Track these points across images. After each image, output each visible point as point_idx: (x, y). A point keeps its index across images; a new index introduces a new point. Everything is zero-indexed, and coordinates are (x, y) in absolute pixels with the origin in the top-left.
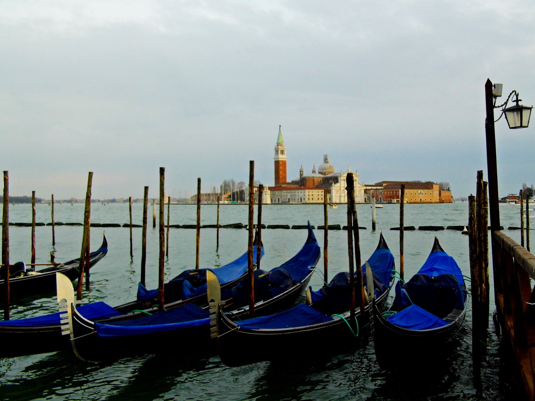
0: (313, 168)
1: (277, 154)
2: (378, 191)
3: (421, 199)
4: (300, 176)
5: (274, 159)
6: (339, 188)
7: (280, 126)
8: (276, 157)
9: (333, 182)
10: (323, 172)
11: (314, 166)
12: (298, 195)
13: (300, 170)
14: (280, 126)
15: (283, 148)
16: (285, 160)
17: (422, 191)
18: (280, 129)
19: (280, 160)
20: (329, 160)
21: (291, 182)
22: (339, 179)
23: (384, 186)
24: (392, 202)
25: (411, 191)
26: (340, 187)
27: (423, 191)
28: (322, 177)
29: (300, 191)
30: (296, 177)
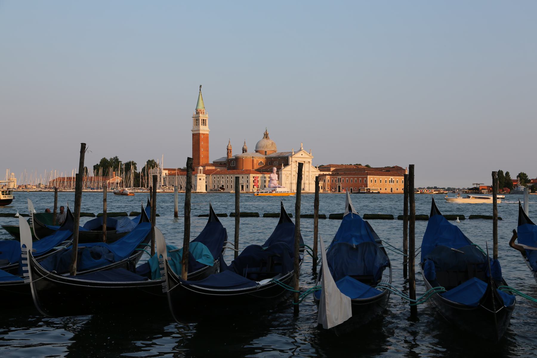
1: (197, 125)
2: (336, 178)
3: (392, 189)
4: (228, 155)
5: (192, 131)
6: (290, 172)
7: (201, 86)
8: (195, 129)
9: (283, 165)
10: (263, 151)
11: (245, 142)
13: (228, 147)
14: (201, 86)
15: (205, 116)
16: (208, 133)
17: (393, 178)
18: (200, 90)
19: (201, 132)
21: (213, 163)
22: (290, 159)
23: (332, 171)
24: (361, 192)
25: (381, 178)
27: (394, 178)
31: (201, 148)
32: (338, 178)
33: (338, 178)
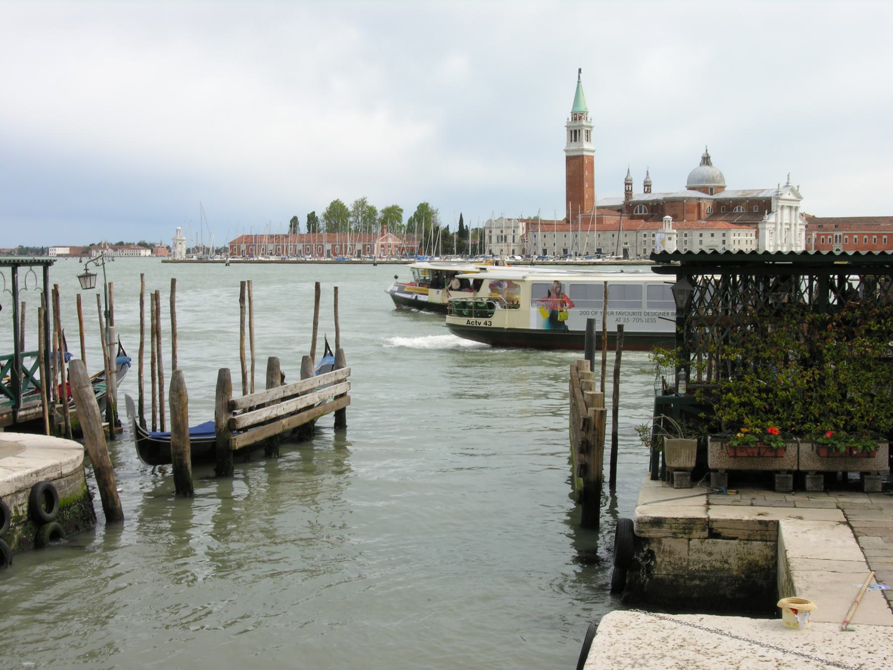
0: (645, 176)
1: (575, 141)
5: (566, 151)
6: (773, 226)
9: (766, 212)
11: (648, 172)
12: (701, 242)
13: (626, 180)
14: (580, 70)
18: (579, 77)
19: (585, 153)
20: (712, 160)
26: (776, 224)
28: (711, 199)
29: (707, 234)
30: (618, 199)
31: (585, 182)
32: (836, 236)
33: (836, 236)
